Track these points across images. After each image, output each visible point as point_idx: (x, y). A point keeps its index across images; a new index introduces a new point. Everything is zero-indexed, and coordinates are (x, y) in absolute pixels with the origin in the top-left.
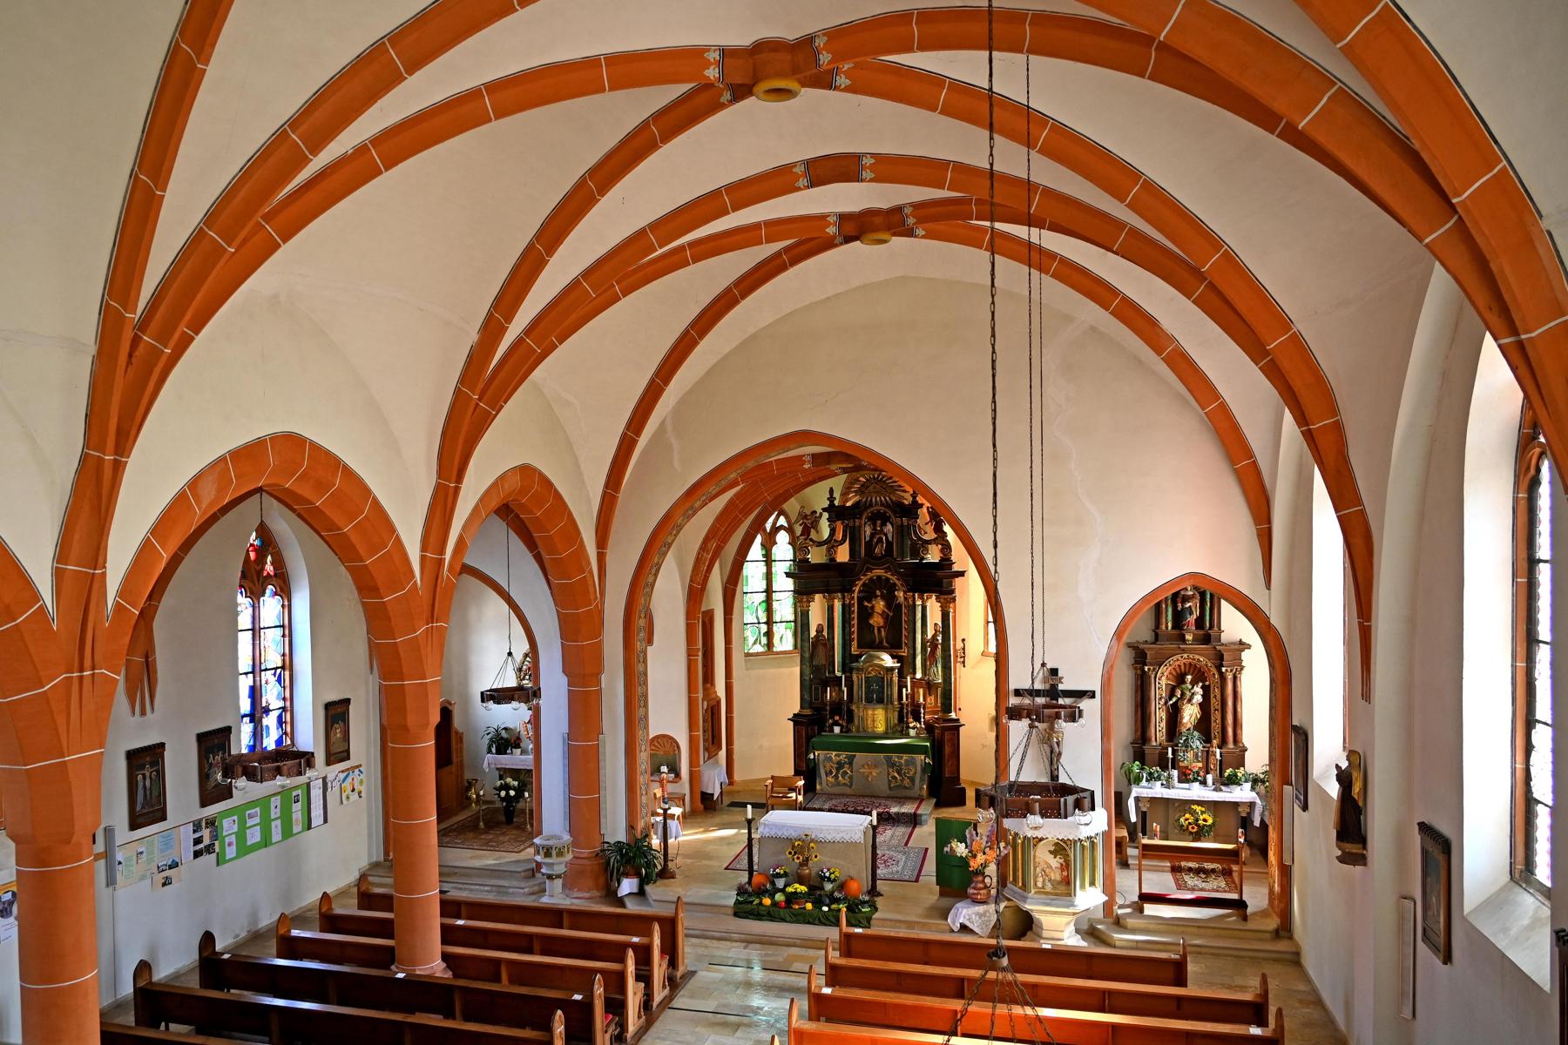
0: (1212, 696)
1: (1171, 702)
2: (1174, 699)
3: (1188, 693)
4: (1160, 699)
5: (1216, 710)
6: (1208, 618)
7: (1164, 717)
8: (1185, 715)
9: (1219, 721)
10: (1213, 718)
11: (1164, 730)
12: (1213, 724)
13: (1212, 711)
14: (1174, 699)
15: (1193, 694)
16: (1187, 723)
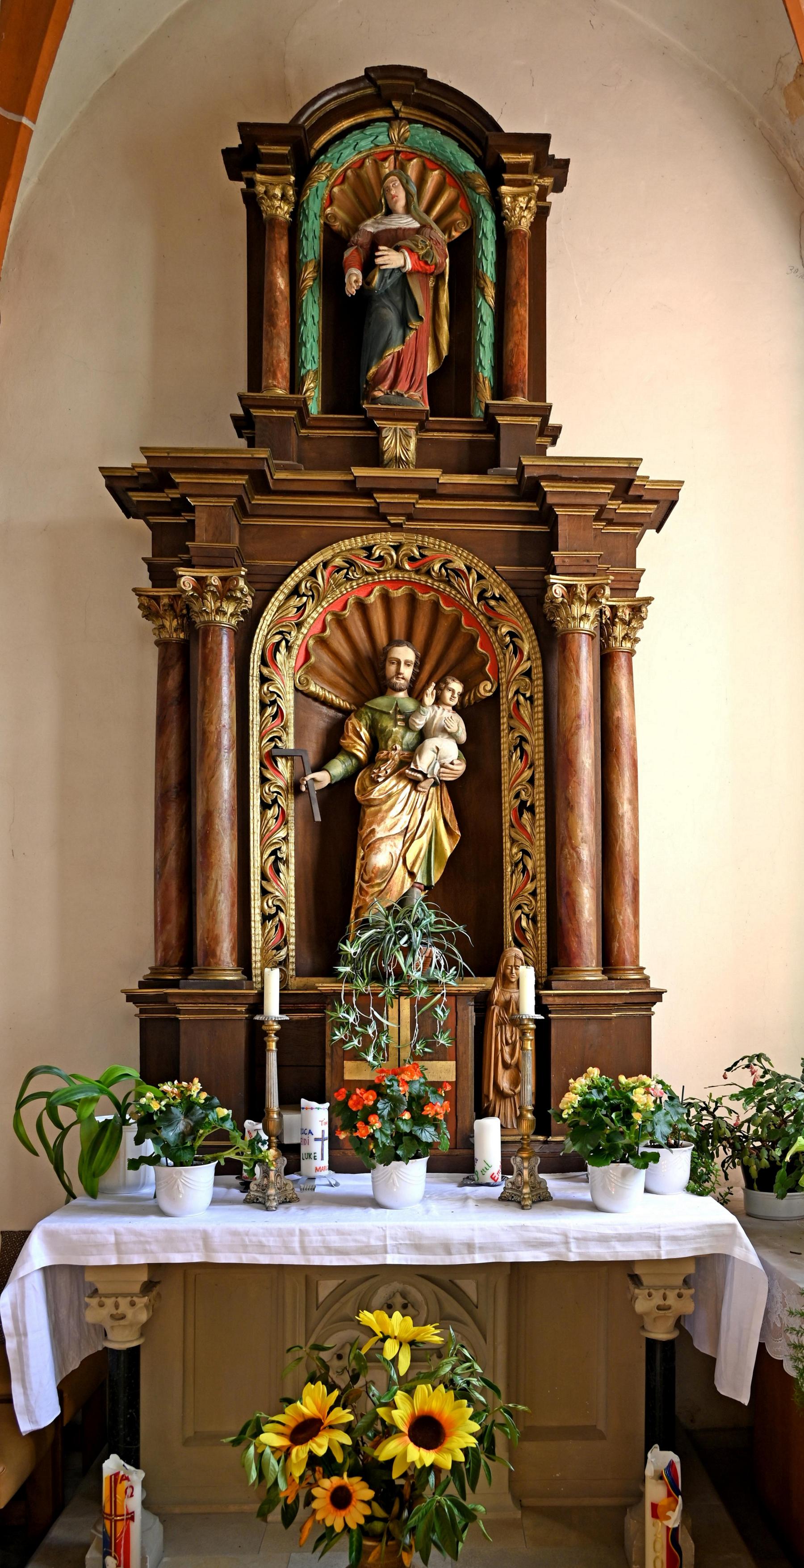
0: (506, 740)
1: (323, 778)
2: (338, 768)
3: (397, 730)
4: (269, 759)
5: (523, 807)
6: (486, 357)
7: (289, 851)
8: (380, 831)
9: (537, 862)
10: (511, 852)
11: (289, 918)
12: (512, 882)
13: (507, 816)
14: (338, 768)
15: (422, 736)
16: (388, 874)
